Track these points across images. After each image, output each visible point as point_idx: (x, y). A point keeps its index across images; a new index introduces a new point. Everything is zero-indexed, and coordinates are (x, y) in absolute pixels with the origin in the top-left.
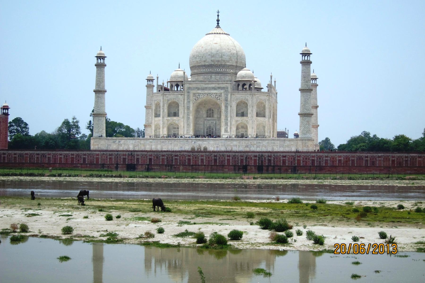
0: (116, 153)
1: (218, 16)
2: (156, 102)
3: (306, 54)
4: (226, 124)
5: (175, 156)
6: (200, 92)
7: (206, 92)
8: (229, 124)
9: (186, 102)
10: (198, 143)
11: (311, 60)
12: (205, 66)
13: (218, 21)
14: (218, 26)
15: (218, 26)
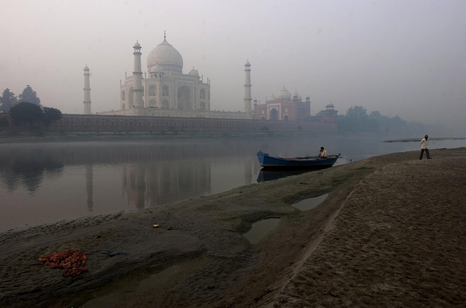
0: (162, 119)
1: (165, 34)
2: (150, 85)
3: (248, 65)
4: (195, 103)
5: (197, 121)
6: (181, 81)
7: (184, 81)
8: (197, 103)
9: (173, 87)
10: (200, 113)
11: (250, 69)
12: (169, 65)
13: (165, 37)
14: (165, 40)
15: (165, 40)
